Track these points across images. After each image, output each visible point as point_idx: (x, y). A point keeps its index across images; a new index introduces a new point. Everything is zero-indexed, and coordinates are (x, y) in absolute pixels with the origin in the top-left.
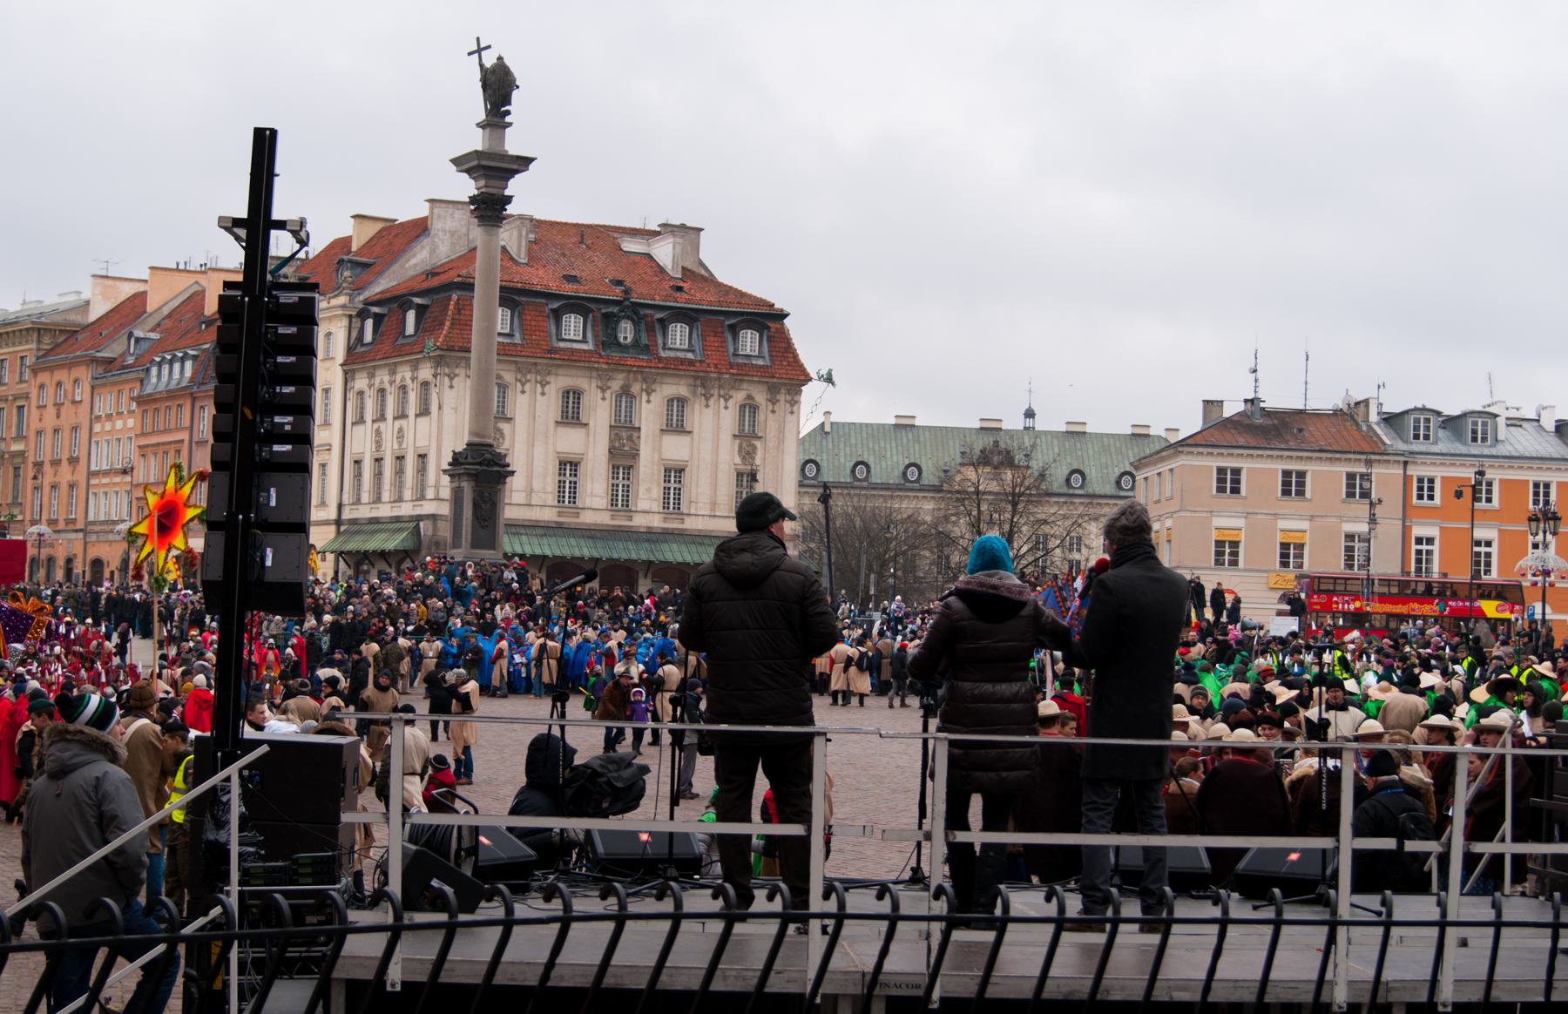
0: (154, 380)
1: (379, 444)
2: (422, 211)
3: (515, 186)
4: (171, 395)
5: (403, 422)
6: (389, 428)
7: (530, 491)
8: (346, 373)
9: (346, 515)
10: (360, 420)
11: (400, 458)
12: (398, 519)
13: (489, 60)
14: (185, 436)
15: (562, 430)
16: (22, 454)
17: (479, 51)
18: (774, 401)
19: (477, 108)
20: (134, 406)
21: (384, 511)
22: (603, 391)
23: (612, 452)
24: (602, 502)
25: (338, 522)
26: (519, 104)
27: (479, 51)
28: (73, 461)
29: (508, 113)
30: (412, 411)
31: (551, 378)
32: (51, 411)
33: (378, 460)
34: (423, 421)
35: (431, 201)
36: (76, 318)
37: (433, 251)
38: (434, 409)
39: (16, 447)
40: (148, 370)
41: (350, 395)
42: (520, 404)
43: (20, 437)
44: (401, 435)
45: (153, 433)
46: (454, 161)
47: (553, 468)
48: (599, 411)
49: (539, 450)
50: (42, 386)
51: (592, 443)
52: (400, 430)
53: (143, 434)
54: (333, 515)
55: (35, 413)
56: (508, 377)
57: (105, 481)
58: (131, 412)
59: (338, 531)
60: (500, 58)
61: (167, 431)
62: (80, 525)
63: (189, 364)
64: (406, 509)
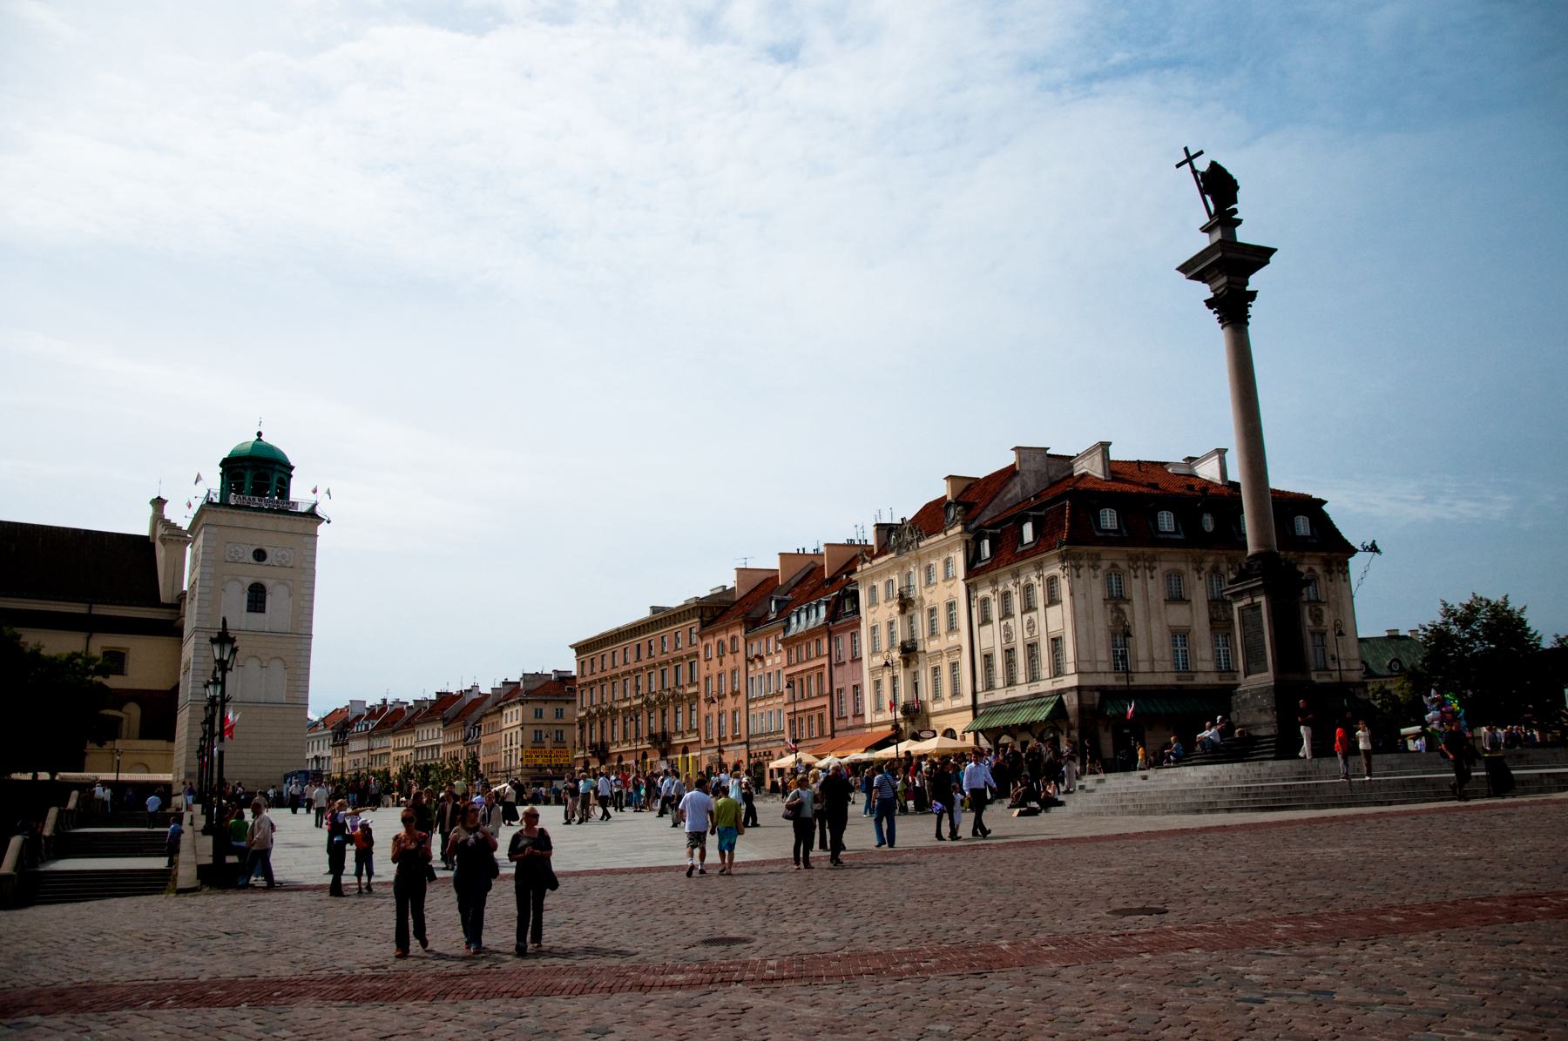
0: (794, 626)
1: (1008, 637)
2: (1010, 459)
3: (1255, 282)
4: (811, 633)
5: (1033, 615)
6: (1018, 622)
7: (1152, 661)
8: (968, 586)
9: (981, 699)
10: (986, 620)
11: (1032, 648)
12: (1037, 696)
13: (1202, 165)
14: (825, 661)
15: (1171, 608)
16: (696, 695)
17: (1189, 159)
18: (1329, 571)
19: (1198, 211)
20: (780, 646)
21: (1021, 691)
22: (1199, 571)
23: (1212, 620)
24: (1210, 666)
25: (975, 707)
26: (1244, 206)
27: (1189, 159)
28: (735, 694)
29: (1235, 211)
30: (1040, 604)
31: (1157, 564)
32: (716, 661)
33: (1009, 653)
34: (1054, 611)
35: (1017, 449)
36: (729, 598)
37: (1023, 487)
38: (1065, 596)
39: (691, 690)
40: (788, 620)
41: (974, 603)
42: (1135, 588)
43: (692, 683)
44: (1031, 625)
45: (798, 663)
46: (1184, 269)
47: (1167, 640)
48: (1199, 592)
49: (1155, 626)
50: (706, 646)
51: (1196, 617)
52: (1030, 621)
53: (789, 665)
54: (968, 701)
55: (703, 665)
56: (1123, 565)
57: (761, 704)
58: (778, 652)
59: (975, 716)
60: (1214, 165)
61: (809, 659)
62: (744, 739)
63: (823, 609)
64: (1045, 686)
